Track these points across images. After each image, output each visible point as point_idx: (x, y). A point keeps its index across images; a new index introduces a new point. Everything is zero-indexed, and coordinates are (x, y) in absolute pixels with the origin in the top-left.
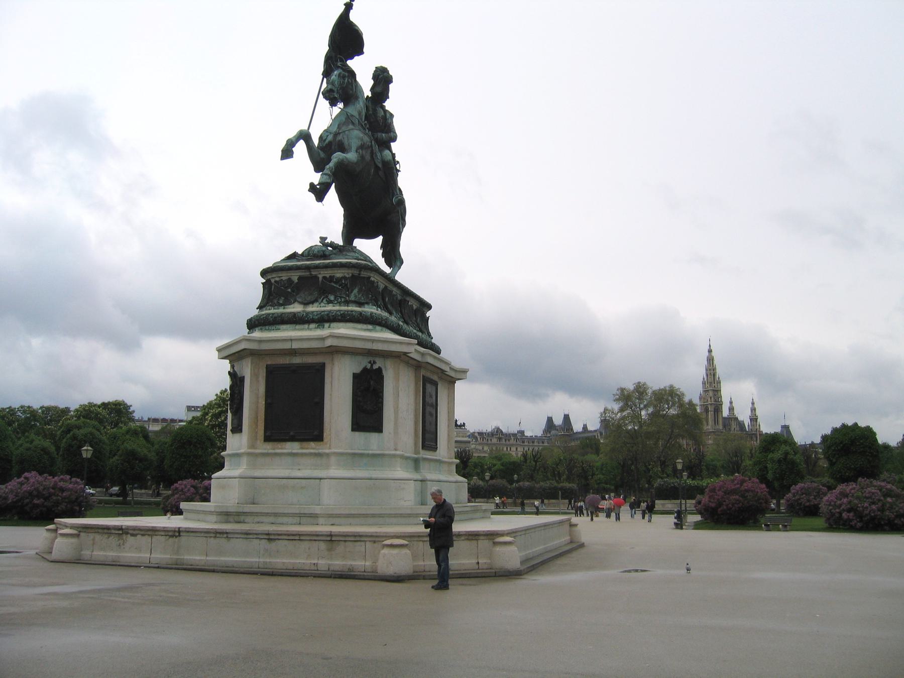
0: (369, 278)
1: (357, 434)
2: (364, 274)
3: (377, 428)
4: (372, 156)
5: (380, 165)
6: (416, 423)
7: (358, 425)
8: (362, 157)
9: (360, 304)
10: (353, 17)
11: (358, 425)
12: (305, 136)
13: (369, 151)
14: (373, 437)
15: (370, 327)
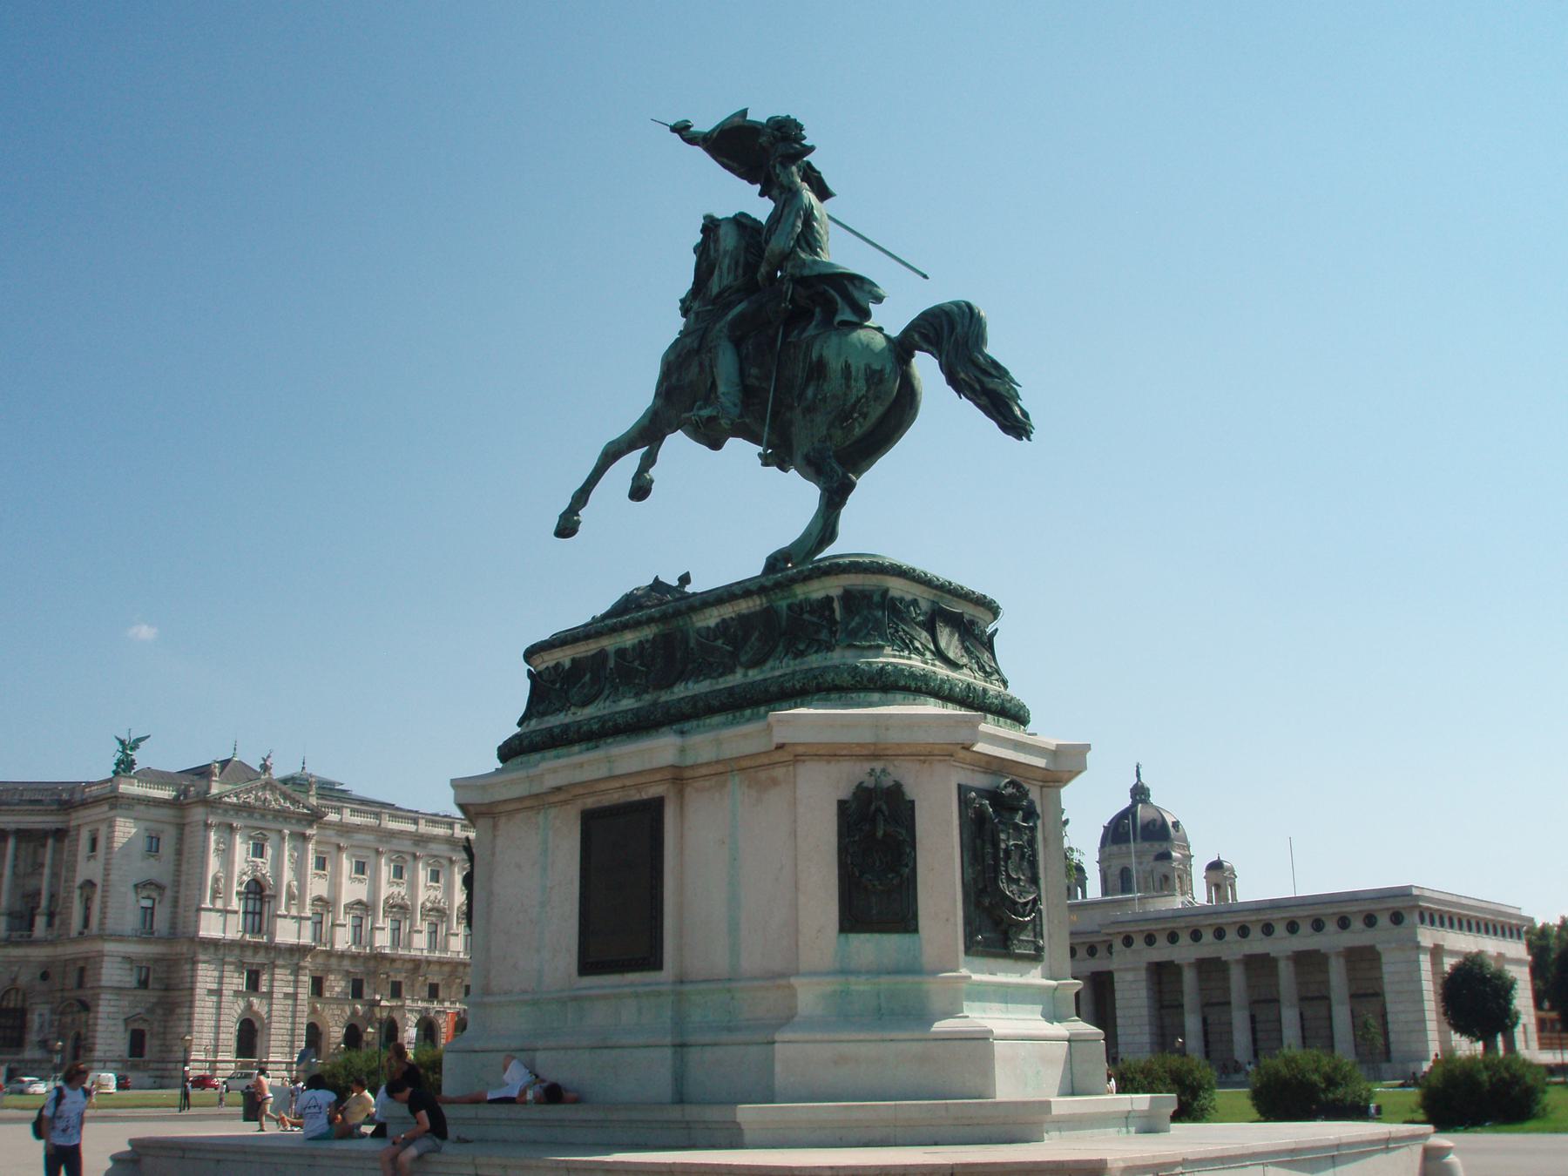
10: (705, 123)
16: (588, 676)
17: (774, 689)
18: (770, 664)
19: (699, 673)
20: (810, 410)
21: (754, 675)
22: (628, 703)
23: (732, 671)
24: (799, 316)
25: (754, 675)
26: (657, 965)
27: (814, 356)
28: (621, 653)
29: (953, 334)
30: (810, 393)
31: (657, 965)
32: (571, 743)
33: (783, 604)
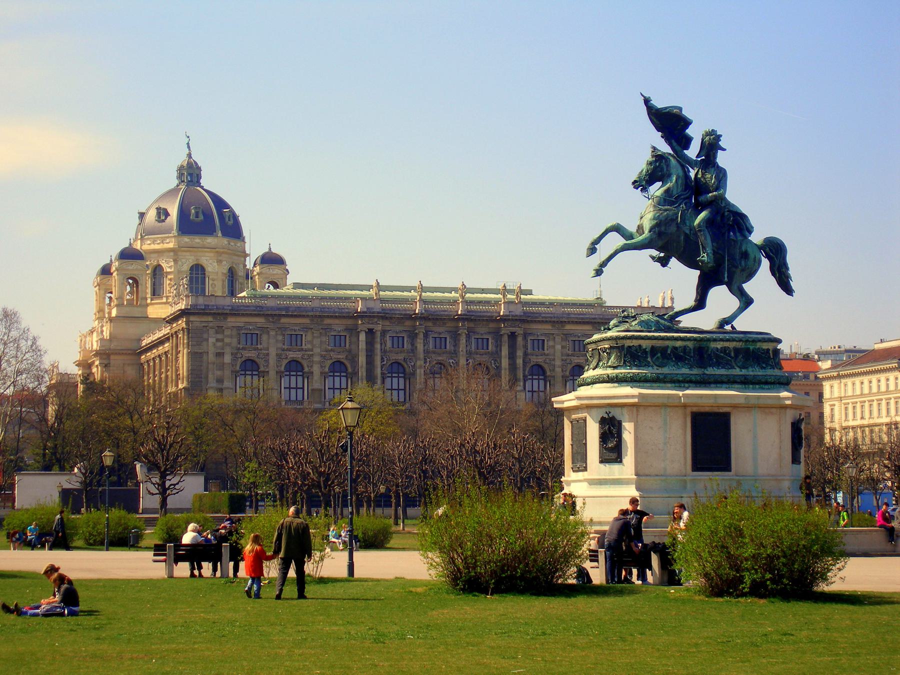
0: (623, 346)
1: (602, 465)
2: (620, 343)
3: (618, 459)
4: (678, 227)
5: (688, 232)
6: (685, 451)
7: (603, 460)
8: (660, 234)
9: (615, 368)
10: (659, 103)
11: (603, 460)
12: (617, 229)
13: (674, 224)
14: (615, 467)
15: (616, 385)
16: (659, 355)
17: (763, 380)
18: (750, 369)
19: (718, 364)
20: (743, 270)
21: (744, 372)
22: (685, 371)
23: (733, 368)
24: (731, 228)
25: (744, 372)
26: (730, 471)
27: (743, 249)
28: (675, 348)
29: (775, 251)
30: (743, 263)
31: (730, 471)
32: (665, 382)
33: (751, 347)
